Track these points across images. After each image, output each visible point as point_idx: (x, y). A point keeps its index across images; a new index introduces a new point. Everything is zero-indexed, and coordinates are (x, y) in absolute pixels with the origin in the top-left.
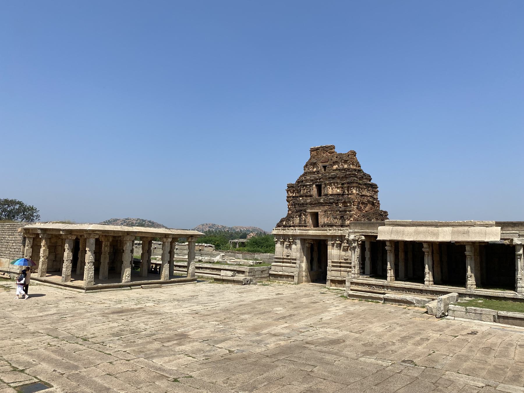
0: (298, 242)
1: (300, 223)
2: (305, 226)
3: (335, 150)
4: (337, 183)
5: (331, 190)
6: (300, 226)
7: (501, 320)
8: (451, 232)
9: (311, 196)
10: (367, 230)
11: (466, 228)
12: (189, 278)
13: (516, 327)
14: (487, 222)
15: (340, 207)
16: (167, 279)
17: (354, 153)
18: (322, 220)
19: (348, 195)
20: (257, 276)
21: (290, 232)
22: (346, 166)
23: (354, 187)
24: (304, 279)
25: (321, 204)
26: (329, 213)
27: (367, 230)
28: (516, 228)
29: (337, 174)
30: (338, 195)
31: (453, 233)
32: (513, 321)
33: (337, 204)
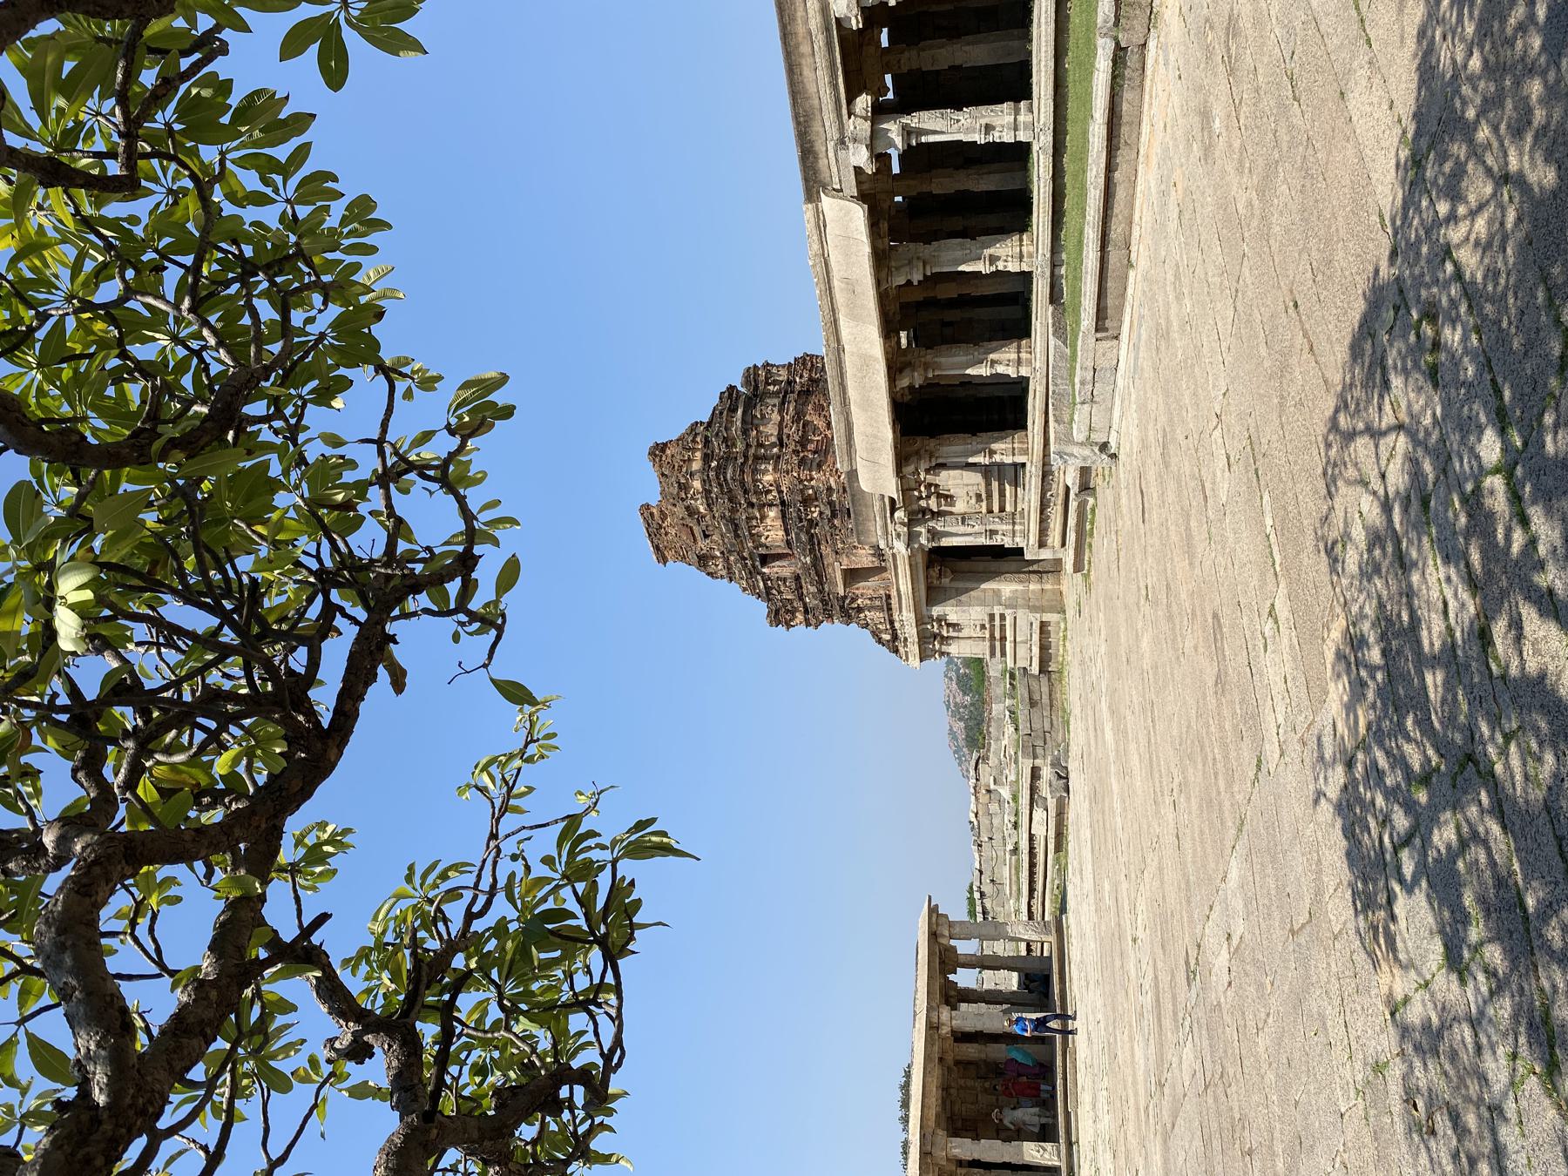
0: (936, 611)
1: (881, 609)
2: (889, 597)
3: (654, 498)
4: (749, 519)
5: (773, 532)
6: (889, 609)
7: (1108, 323)
8: (852, 324)
9: (797, 578)
11: (836, 283)
12: (1052, 938)
13: (1130, 291)
14: (810, 226)
15: (821, 513)
17: (657, 451)
18: (864, 559)
19: (780, 492)
21: (910, 630)
22: (697, 484)
23: (755, 481)
24: (1048, 587)
25: (818, 561)
27: (877, 507)
28: (819, 147)
29: (723, 517)
30: (783, 516)
31: (854, 317)
32: (1110, 297)
33: (812, 523)
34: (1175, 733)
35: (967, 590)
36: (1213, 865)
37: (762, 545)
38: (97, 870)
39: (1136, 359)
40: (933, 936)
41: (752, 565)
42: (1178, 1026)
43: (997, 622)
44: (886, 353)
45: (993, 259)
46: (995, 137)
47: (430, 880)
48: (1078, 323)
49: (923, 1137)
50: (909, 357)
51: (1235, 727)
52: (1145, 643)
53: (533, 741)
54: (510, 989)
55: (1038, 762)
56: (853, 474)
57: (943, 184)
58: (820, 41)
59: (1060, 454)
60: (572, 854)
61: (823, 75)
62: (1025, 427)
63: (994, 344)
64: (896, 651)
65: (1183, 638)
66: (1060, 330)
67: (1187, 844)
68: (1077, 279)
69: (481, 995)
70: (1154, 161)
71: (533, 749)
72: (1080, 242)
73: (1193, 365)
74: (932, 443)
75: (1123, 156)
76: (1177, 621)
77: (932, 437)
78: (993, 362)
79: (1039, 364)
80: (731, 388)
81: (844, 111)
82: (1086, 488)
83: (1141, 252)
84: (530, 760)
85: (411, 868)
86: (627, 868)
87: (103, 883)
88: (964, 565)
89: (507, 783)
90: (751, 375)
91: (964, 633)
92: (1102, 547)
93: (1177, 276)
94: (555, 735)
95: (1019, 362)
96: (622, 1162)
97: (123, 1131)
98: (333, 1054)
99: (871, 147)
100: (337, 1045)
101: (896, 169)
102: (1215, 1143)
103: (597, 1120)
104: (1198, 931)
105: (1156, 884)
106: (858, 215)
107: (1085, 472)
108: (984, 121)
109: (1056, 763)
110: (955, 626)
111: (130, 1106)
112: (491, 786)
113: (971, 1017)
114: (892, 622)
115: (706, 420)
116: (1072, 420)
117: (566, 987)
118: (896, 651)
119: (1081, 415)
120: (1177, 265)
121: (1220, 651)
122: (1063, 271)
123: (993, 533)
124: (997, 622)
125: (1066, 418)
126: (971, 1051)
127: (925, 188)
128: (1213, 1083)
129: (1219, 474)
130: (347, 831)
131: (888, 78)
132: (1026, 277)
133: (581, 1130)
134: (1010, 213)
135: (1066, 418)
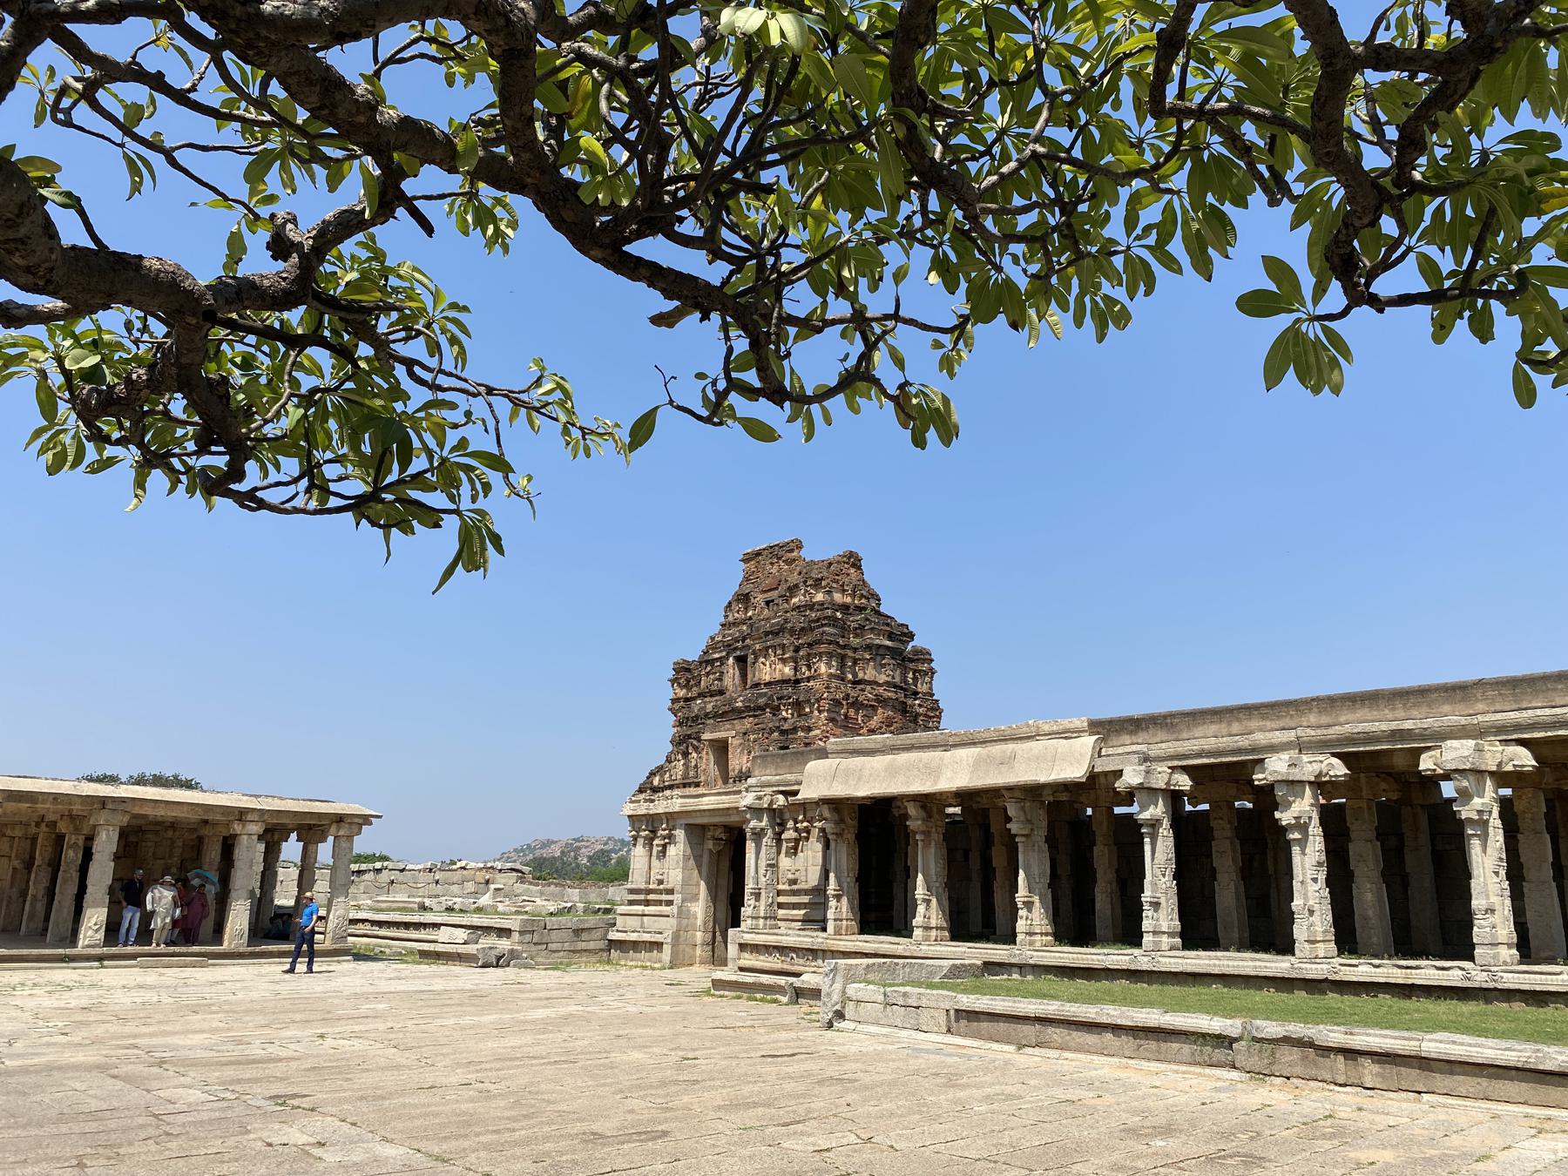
0: (680, 834)
1: (685, 776)
2: (697, 785)
3: (807, 554)
5: (769, 670)
6: (685, 786)
7: (963, 1022)
9: (721, 692)
10: (789, 777)
11: (1010, 746)
13: (995, 1046)
14: (1066, 723)
15: (785, 719)
16: (238, 946)
17: (853, 560)
18: (738, 761)
20: (552, 946)
21: (661, 806)
22: (820, 597)
23: (820, 655)
24: (698, 951)
25: (737, 714)
26: (752, 737)
27: (789, 777)
30: (784, 682)
31: (977, 763)
33: (776, 710)
34: (543, 1087)
35: (699, 867)
36: (400, 1126)
37: (756, 658)
38: (501, 22)
39: (928, 1051)
40: (340, 819)
41: (737, 647)
42: (226, 1084)
43: (664, 897)
44: (941, 794)
45: (1029, 905)
46: (1148, 913)
47: (450, 326)
48: (965, 991)
49: (123, 800)
50: (936, 816)
51: (547, 1154)
52: (637, 1055)
53: (584, 435)
54: (331, 400)
55: (516, 936)
56: (823, 754)
57: (1103, 857)
58: (1243, 742)
59: (835, 970)
60: (469, 469)
61: (1210, 743)
62: (862, 932)
63: (946, 903)
64: (641, 791)
65: (642, 1098)
66: (957, 971)
67: (423, 1098)
68: (1009, 992)
69: (327, 370)
70: (1123, 1075)
71: (576, 433)
72: (1044, 996)
73: (921, 1112)
74: (851, 836)
75: (1127, 1042)
76: (660, 1091)
77: (857, 836)
78: (928, 902)
79: (925, 949)
80: (911, 636)
81: (1176, 763)
82: (799, 994)
83: (1032, 1058)
84: (566, 432)
85: (465, 309)
86: (451, 524)
87: (488, 27)
88: (725, 865)
89: (543, 407)
90: (923, 656)
91: (655, 862)
92: (737, 1010)
93: (1010, 1097)
94: (588, 456)
95: (927, 928)
96: (135, 501)
97: (233, 26)
98: (280, 221)
99: (1141, 787)
100: (289, 226)
101: (1118, 810)
102: (94, 1124)
103: (183, 478)
104: (329, 1109)
105: (382, 1062)
106: (1076, 771)
107: (815, 994)
108: (1163, 901)
109: (513, 955)
110: (663, 852)
111: (258, 34)
112: (541, 391)
113: (249, 854)
114: (671, 787)
115: (882, 609)
116: (869, 983)
117: (329, 455)
118: (641, 791)
119: (872, 992)
120: (1020, 1097)
121: (623, 1138)
122: (1015, 976)
123: (757, 896)
124: (664, 897)
125: (870, 977)
126: (213, 854)
127: (1099, 839)
128: (161, 1126)
129: (811, 1139)
130: (506, 248)
131: (1206, 807)
132: (1010, 938)
133: (175, 462)
134: (1074, 925)
135: (870, 977)
